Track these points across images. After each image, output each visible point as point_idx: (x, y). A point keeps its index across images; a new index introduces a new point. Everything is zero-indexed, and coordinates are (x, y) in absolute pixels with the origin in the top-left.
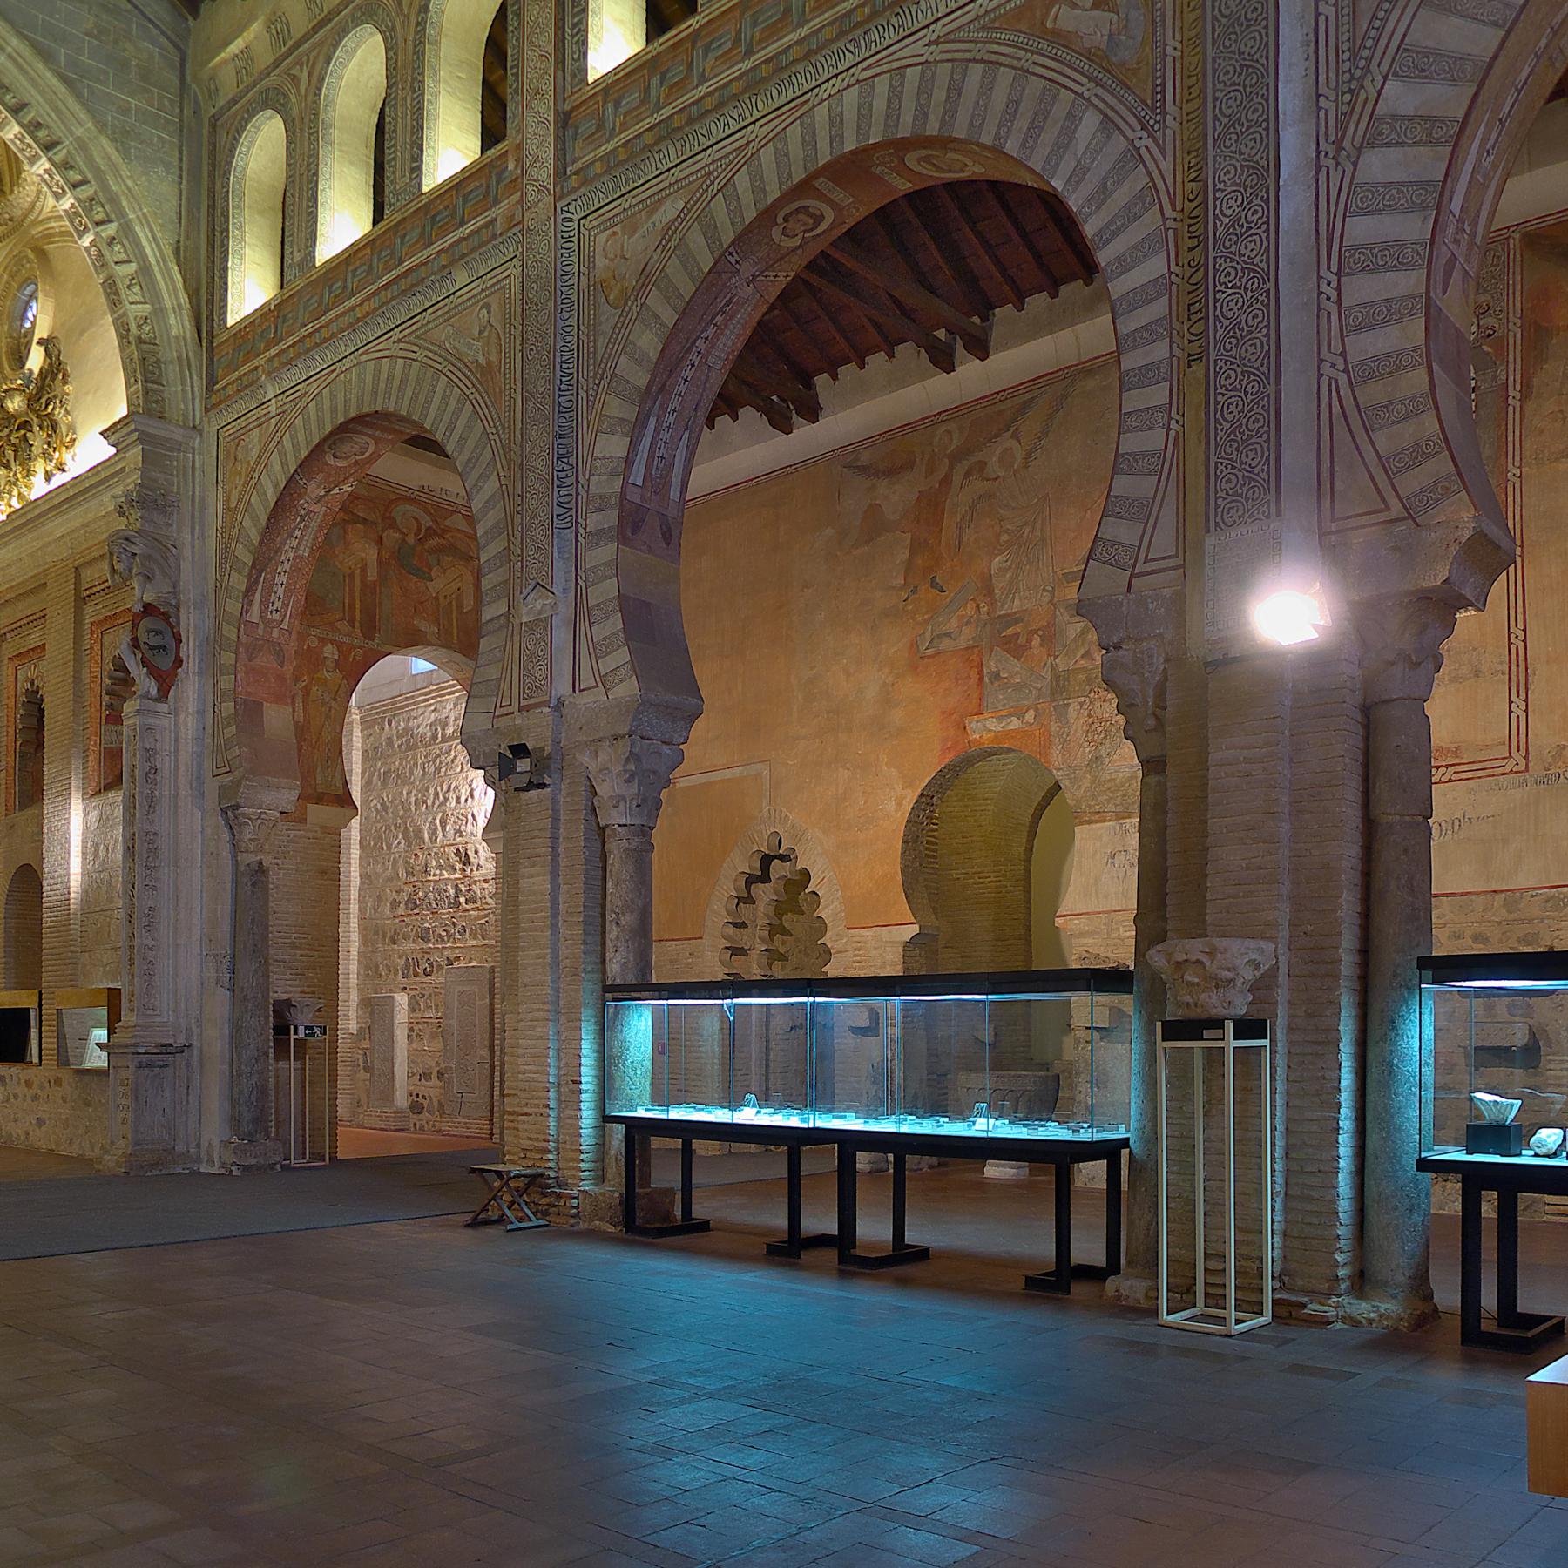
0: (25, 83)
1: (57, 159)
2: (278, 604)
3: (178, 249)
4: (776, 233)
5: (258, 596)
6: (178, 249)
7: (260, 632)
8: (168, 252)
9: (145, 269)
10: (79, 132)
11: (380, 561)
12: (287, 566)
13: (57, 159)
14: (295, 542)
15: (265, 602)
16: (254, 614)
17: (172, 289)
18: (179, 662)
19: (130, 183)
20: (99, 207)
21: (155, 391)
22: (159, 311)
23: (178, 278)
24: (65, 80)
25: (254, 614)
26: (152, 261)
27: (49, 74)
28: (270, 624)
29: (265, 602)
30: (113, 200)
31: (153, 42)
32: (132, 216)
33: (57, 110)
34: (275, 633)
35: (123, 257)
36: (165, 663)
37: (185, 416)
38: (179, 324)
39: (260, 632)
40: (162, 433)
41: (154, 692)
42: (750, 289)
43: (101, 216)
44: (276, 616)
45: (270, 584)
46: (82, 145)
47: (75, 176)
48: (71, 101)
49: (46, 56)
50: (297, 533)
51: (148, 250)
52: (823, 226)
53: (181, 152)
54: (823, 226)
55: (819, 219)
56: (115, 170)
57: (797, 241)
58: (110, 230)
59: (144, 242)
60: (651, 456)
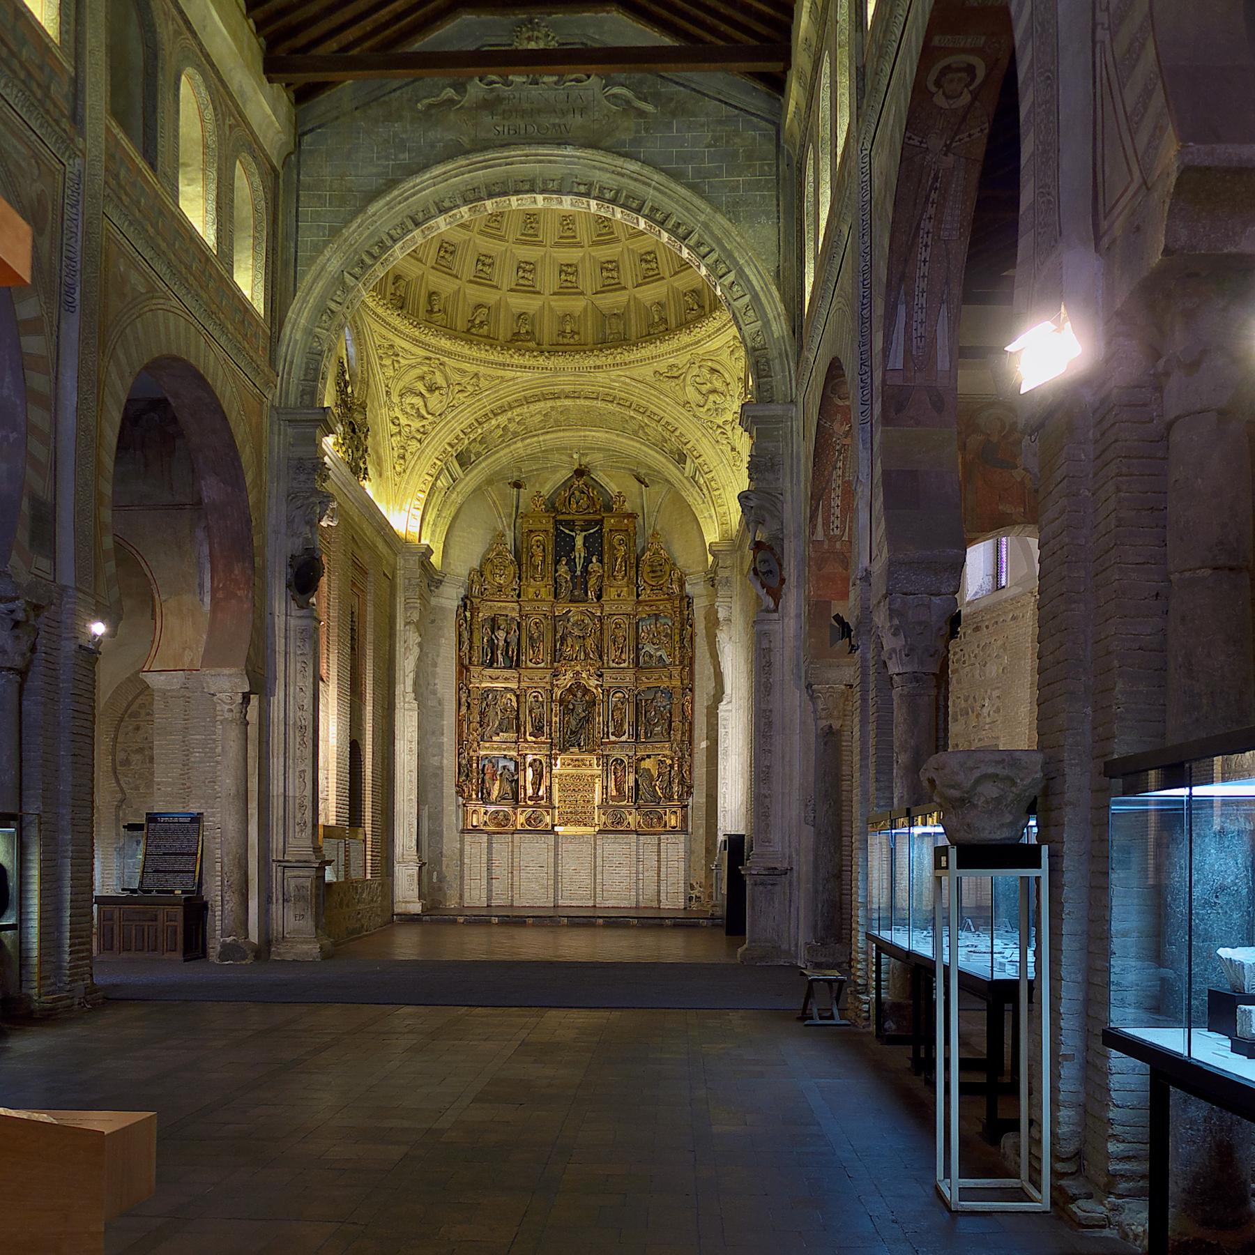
0: (666, 200)
1: (692, 243)
2: (837, 523)
3: (778, 272)
4: (939, 100)
5: (820, 520)
6: (778, 272)
7: (826, 547)
8: (769, 279)
9: (755, 297)
10: (702, 218)
11: (964, 464)
12: (839, 491)
13: (692, 243)
14: (840, 472)
15: (826, 523)
16: (820, 535)
17: (774, 305)
18: (783, 581)
19: (738, 239)
20: (724, 263)
21: (766, 383)
22: (767, 324)
23: (776, 294)
24: (692, 187)
25: (820, 535)
26: (758, 288)
27: (679, 188)
28: (832, 539)
29: (826, 523)
30: (730, 255)
31: (755, 128)
32: (742, 262)
33: (687, 209)
34: (838, 545)
35: (741, 293)
36: (774, 583)
37: (785, 395)
38: (780, 328)
39: (826, 547)
40: (767, 413)
41: (772, 605)
42: (951, 158)
43: (724, 270)
44: (837, 532)
45: (828, 508)
46: (706, 226)
47: (704, 250)
48: (698, 202)
49: (675, 176)
50: (840, 464)
51: (755, 283)
52: (981, 73)
53: (778, 200)
54: (981, 73)
55: (971, 69)
56: (727, 232)
57: (966, 98)
58: (731, 277)
59: (752, 277)
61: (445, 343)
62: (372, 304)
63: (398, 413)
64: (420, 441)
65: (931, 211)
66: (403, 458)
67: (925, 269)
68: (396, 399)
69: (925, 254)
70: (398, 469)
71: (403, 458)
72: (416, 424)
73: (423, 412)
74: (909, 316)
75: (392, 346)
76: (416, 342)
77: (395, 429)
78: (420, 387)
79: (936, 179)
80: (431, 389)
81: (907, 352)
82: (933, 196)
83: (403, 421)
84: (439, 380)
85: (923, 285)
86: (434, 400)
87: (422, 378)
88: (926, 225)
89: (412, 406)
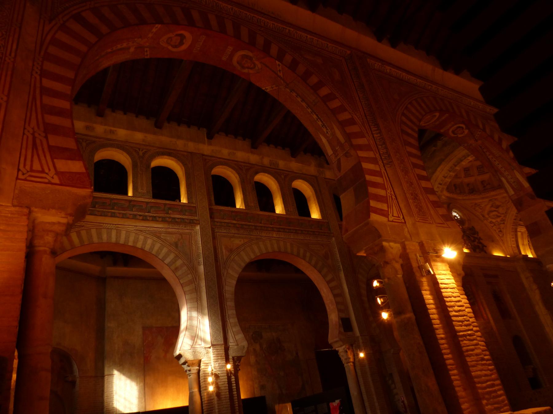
57: (466, 131)
60: (511, 185)
61: (492, 193)
62: (460, 198)
63: (490, 220)
64: (504, 224)
65: (488, 153)
66: (500, 231)
67: (500, 166)
68: (487, 216)
69: (497, 163)
70: (501, 235)
71: (500, 231)
72: (499, 220)
73: (499, 215)
74: (506, 179)
75: (476, 204)
76: (483, 198)
77: (492, 225)
78: (493, 209)
79: (481, 147)
80: (498, 207)
81: (513, 188)
82: (485, 150)
83: (494, 221)
84: (498, 203)
85: (503, 169)
86: (500, 210)
87: (492, 206)
88: (490, 157)
89: (494, 215)
